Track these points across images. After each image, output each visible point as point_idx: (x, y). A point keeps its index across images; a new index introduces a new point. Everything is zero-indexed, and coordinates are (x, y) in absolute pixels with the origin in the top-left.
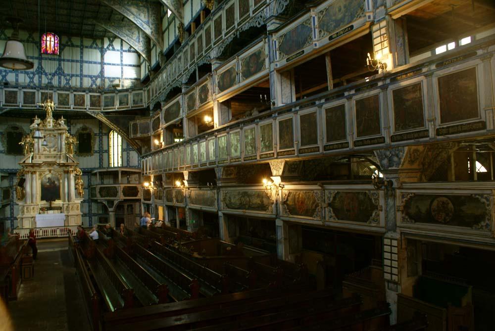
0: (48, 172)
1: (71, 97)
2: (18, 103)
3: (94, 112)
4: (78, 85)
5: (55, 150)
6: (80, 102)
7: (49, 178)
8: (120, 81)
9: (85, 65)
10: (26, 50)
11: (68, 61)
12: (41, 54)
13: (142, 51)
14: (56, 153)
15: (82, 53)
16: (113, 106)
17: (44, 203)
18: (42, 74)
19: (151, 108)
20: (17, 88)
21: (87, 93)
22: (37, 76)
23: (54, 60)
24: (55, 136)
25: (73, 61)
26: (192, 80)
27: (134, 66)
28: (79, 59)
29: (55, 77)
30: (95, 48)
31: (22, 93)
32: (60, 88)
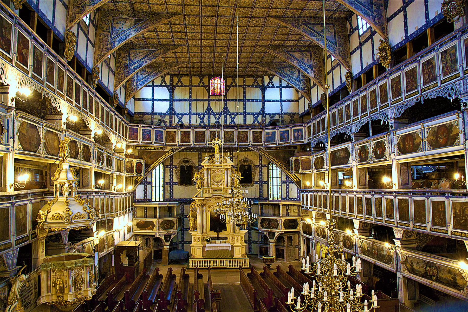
1: (236, 135)
4: (242, 122)
6: (243, 138)
8: (280, 116)
10: (198, 92)
11: (233, 100)
12: (209, 97)
15: (245, 92)
18: (210, 114)
19: (313, 145)
20: (190, 128)
22: (206, 116)
24: (222, 171)
26: (364, 132)
30: (256, 87)
32: (226, 127)
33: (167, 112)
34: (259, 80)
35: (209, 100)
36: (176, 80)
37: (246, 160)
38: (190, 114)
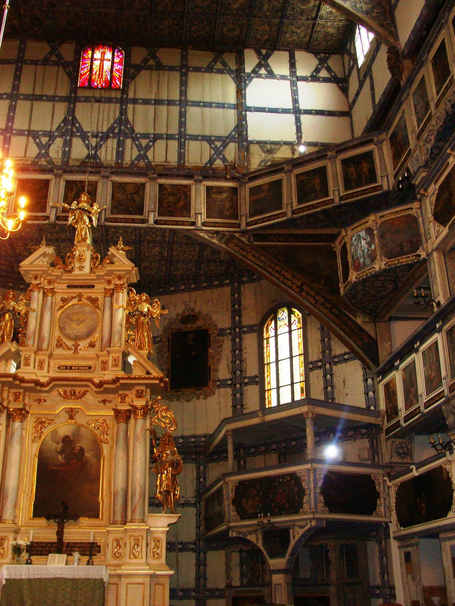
1: (151, 193)
3: (217, 232)
4: (173, 159)
5: (92, 345)
7: (66, 440)
9: (193, 112)
10: (39, 78)
11: (146, 102)
12: (74, 89)
13: (367, 13)
15: (184, 84)
16: (280, 208)
17: (45, 531)
18: (72, 135)
22: (59, 142)
23: (109, 100)
24: (94, 301)
25: (158, 102)
27: (330, 113)
28: (176, 96)
29: (110, 141)
30: (220, 72)
35: (72, 100)
37: (189, 317)
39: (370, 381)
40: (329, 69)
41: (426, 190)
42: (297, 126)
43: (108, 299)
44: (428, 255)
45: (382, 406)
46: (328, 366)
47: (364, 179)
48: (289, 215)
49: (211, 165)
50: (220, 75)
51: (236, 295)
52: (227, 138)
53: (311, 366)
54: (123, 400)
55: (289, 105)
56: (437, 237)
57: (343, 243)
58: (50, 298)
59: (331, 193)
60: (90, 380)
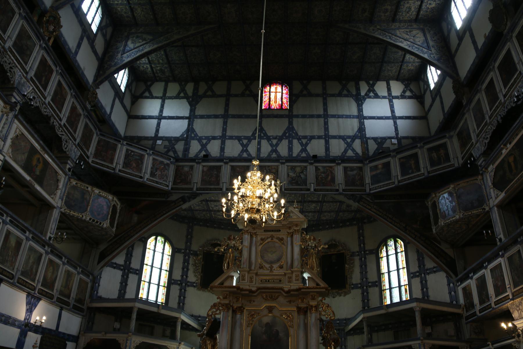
0: (266, 312)
2: (222, 185)
3: (352, 195)
5: (281, 267)
7: (267, 324)
9: (332, 122)
13: (438, 60)
14: (282, 272)
15: (325, 105)
16: (390, 179)
21: (338, 164)
24: (281, 240)
25: (312, 116)
29: (283, 141)
31: (228, 167)
33: (182, 135)
34: (351, 87)
36: (203, 88)
38: (223, 138)
39: (451, 285)
40: (411, 91)
41: (487, 169)
42: (395, 127)
43: (289, 239)
44: (490, 209)
45: (462, 301)
46: (423, 275)
47: (442, 161)
48: (396, 183)
49: (346, 153)
50: (346, 98)
51: (361, 231)
52: (354, 136)
53: (412, 275)
54: (302, 301)
55: (389, 114)
56: (496, 198)
57: (433, 201)
58: (254, 238)
59: (422, 170)
60: (282, 289)
